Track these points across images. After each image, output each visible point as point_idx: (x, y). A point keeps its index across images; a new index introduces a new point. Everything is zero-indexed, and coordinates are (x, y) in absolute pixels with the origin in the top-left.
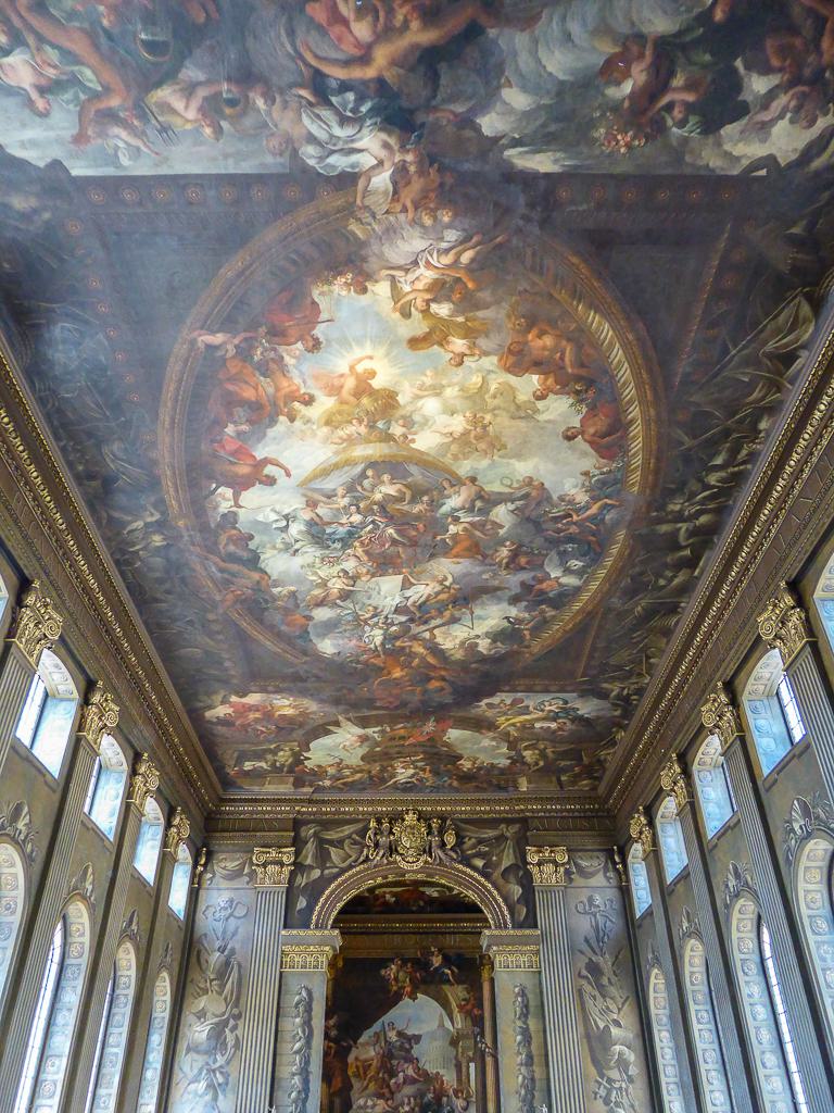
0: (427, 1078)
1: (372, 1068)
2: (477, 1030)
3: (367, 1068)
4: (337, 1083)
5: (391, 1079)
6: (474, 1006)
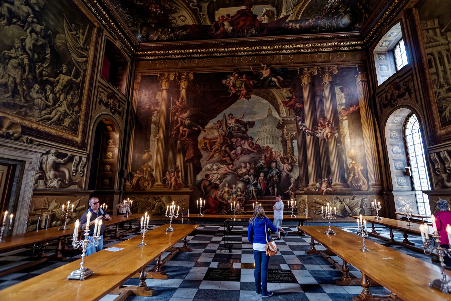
0: (260, 150)
1: (216, 143)
2: (299, 118)
3: (212, 144)
4: (190, 153)
5: (231, 151)
6: (296, 102)
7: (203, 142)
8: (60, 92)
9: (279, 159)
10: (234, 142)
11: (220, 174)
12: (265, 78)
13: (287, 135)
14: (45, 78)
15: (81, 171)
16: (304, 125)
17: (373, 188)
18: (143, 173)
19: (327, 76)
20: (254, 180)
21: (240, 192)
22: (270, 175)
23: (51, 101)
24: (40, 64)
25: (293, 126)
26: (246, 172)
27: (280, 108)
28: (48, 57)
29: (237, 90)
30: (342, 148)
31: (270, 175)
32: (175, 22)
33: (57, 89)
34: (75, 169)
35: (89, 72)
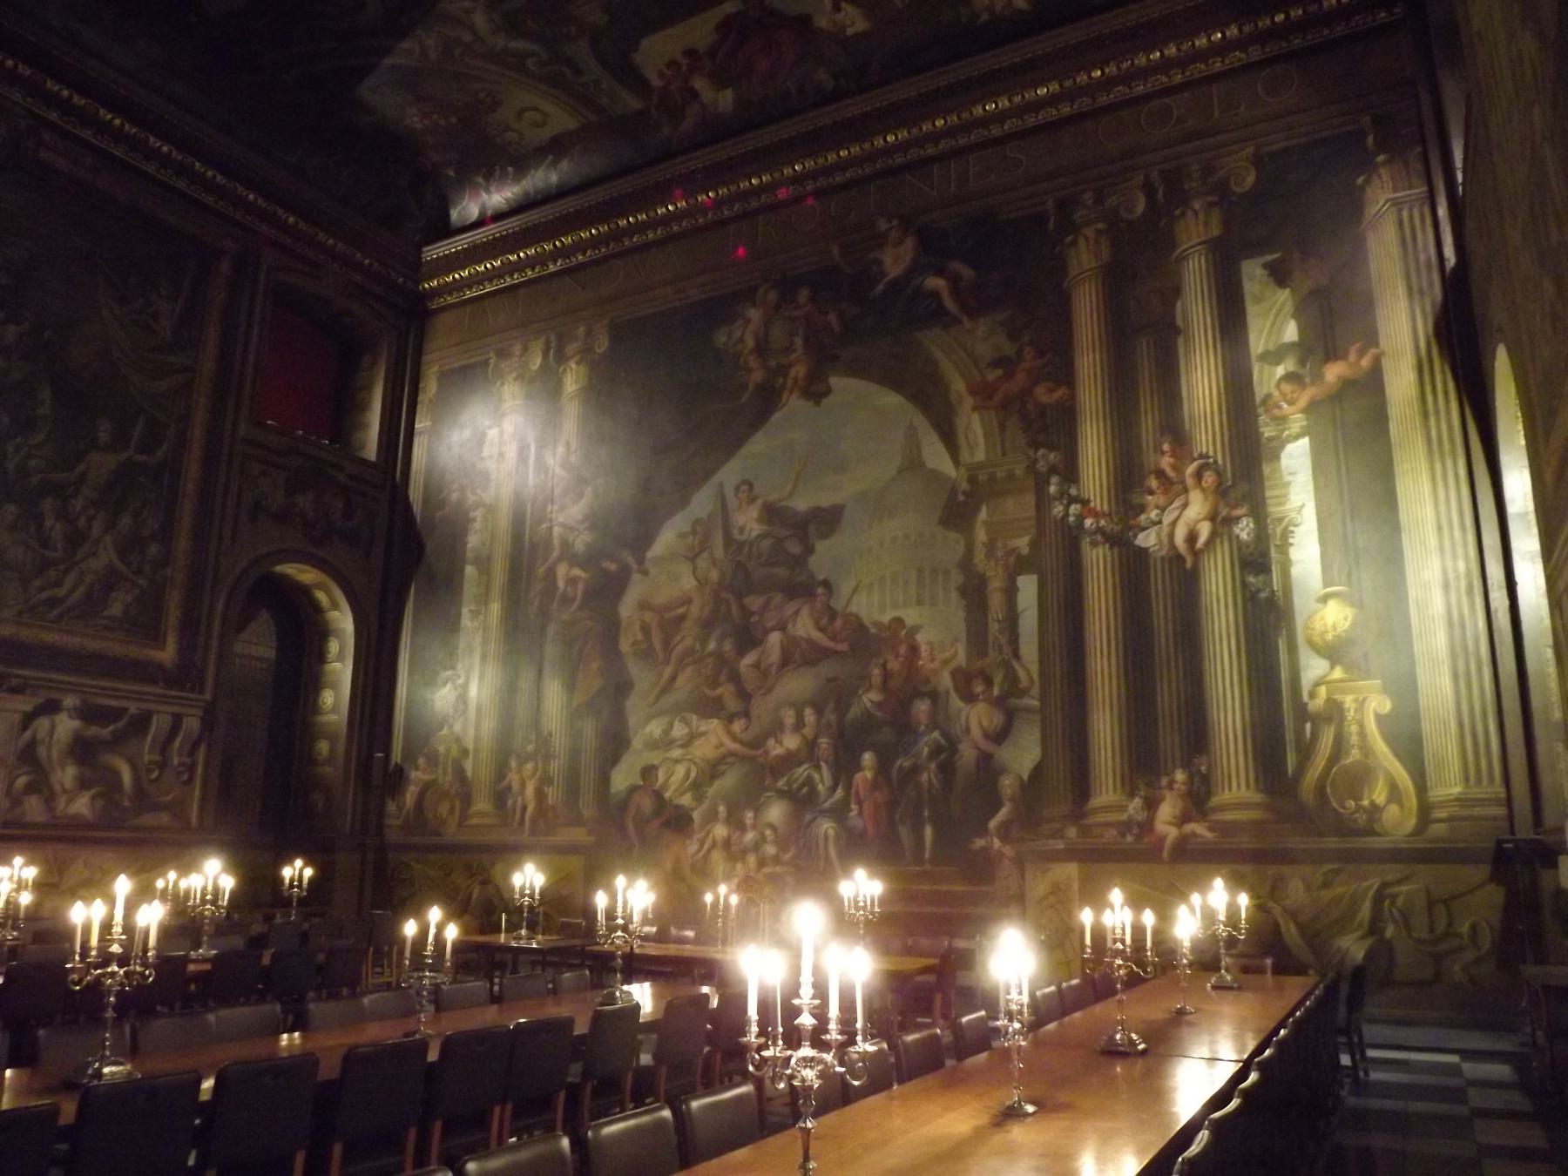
1: (688, 624)
7: (637, 627)
8: (92, 512)
9: (946, 681)
10: (752, 614)
11: (695, 764)
12: (895, 283)
13: (986, 555)
14: (35, 480)
15: (181, 764)
16: (1073, 491)
17: (1451, 819)
18: (436, 764)
19: (1196, 213)
20: (833, 789)
21: (776, 842)
22: (904, 762)
23: (59, 546)
24: (18, 440)
25: (1020, 507)
26: (798, 749)
27: (961, 422)
28: (43, 411)
29: (773, 363)
30: (1272, 602)
31: (904, 762)
32: (511, 136)
33: (78, 504)
34: (157, 757)
35: (200, 417)
